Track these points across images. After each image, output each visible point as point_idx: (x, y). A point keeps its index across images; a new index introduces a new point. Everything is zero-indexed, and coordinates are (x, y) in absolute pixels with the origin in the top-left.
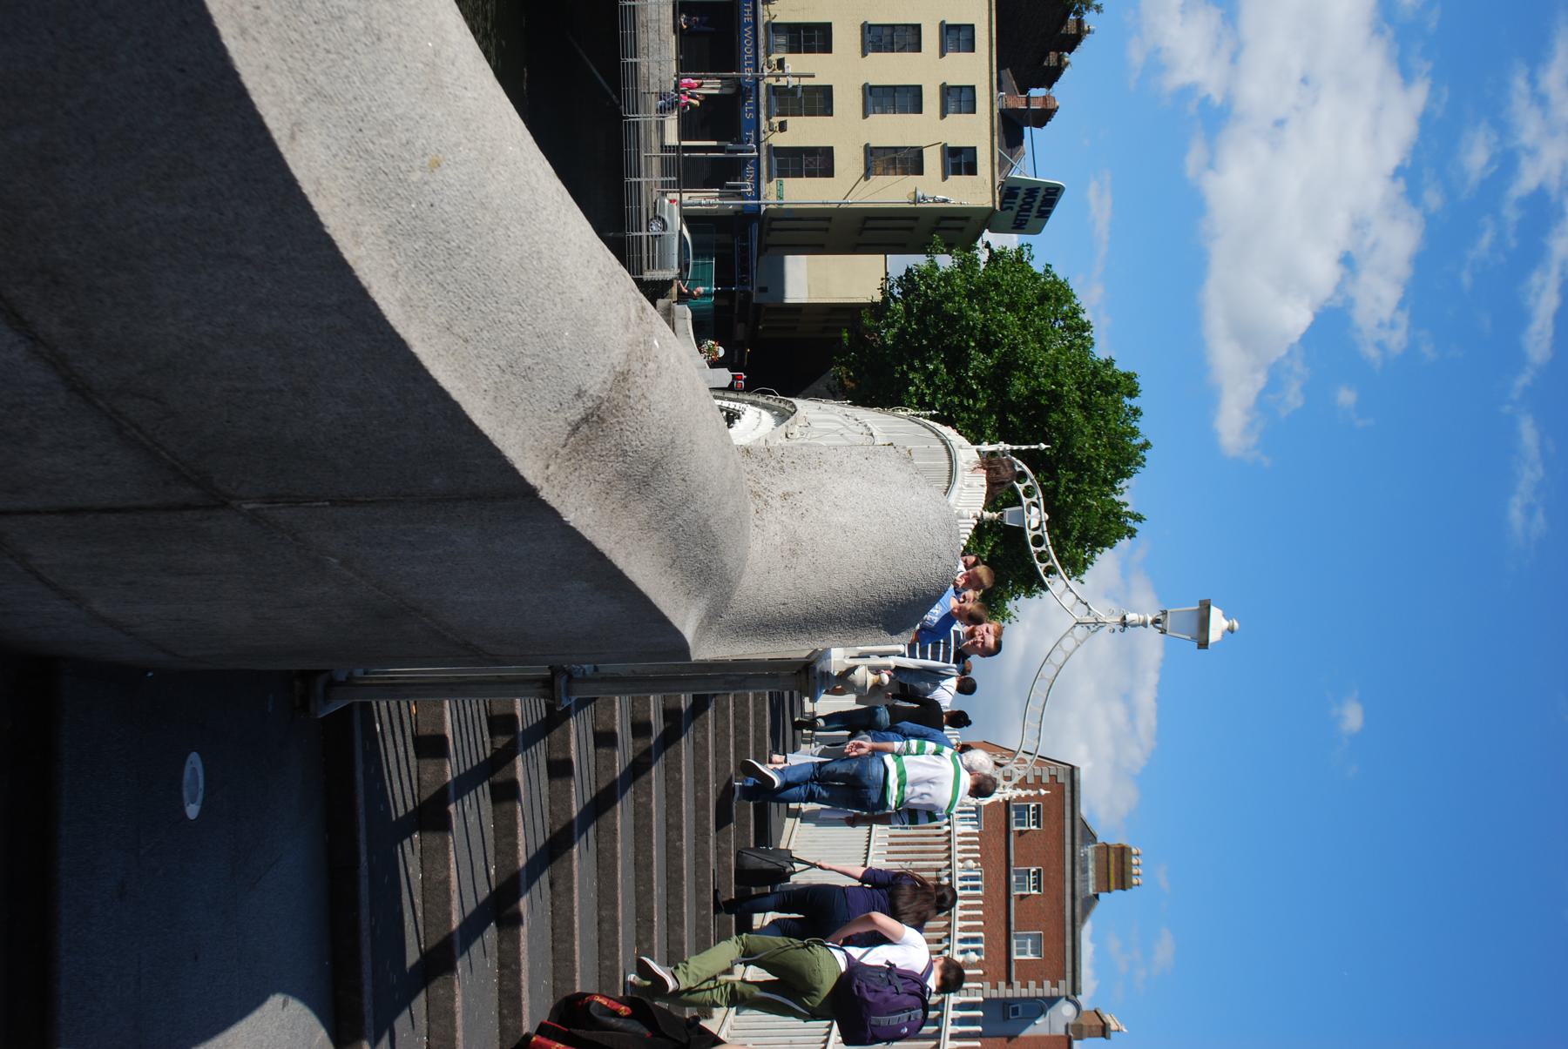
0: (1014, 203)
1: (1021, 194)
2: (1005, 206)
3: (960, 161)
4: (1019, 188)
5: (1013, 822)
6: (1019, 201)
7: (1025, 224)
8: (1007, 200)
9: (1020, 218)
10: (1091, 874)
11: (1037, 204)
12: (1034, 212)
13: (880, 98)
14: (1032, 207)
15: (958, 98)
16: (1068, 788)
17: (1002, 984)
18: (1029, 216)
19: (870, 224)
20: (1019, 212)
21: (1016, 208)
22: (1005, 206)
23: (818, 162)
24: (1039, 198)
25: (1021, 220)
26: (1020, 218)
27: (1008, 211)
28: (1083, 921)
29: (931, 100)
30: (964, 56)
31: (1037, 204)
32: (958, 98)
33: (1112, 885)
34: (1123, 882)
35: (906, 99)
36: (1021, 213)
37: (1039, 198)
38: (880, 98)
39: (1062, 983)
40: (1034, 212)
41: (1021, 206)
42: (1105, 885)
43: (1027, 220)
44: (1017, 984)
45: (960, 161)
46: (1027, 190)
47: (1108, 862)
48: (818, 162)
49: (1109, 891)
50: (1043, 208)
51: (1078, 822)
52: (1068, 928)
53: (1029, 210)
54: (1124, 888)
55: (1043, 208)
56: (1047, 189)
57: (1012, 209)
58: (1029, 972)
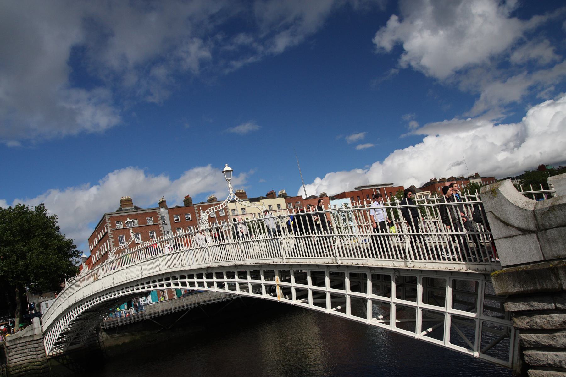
5: (122, 228)
10: (129, 208)
16: (111, 216)
17: (160, 226)
28: (141, 209)
33: (131, 203)
34: (130, 200)
39: (157, 212)
42: (131, 204)
44: (159, 222)
47: (126, 204)
49: (133, 203)
51: (117, 212)
52: (144, 212)
54: (131, 200)
58: (156, 220)
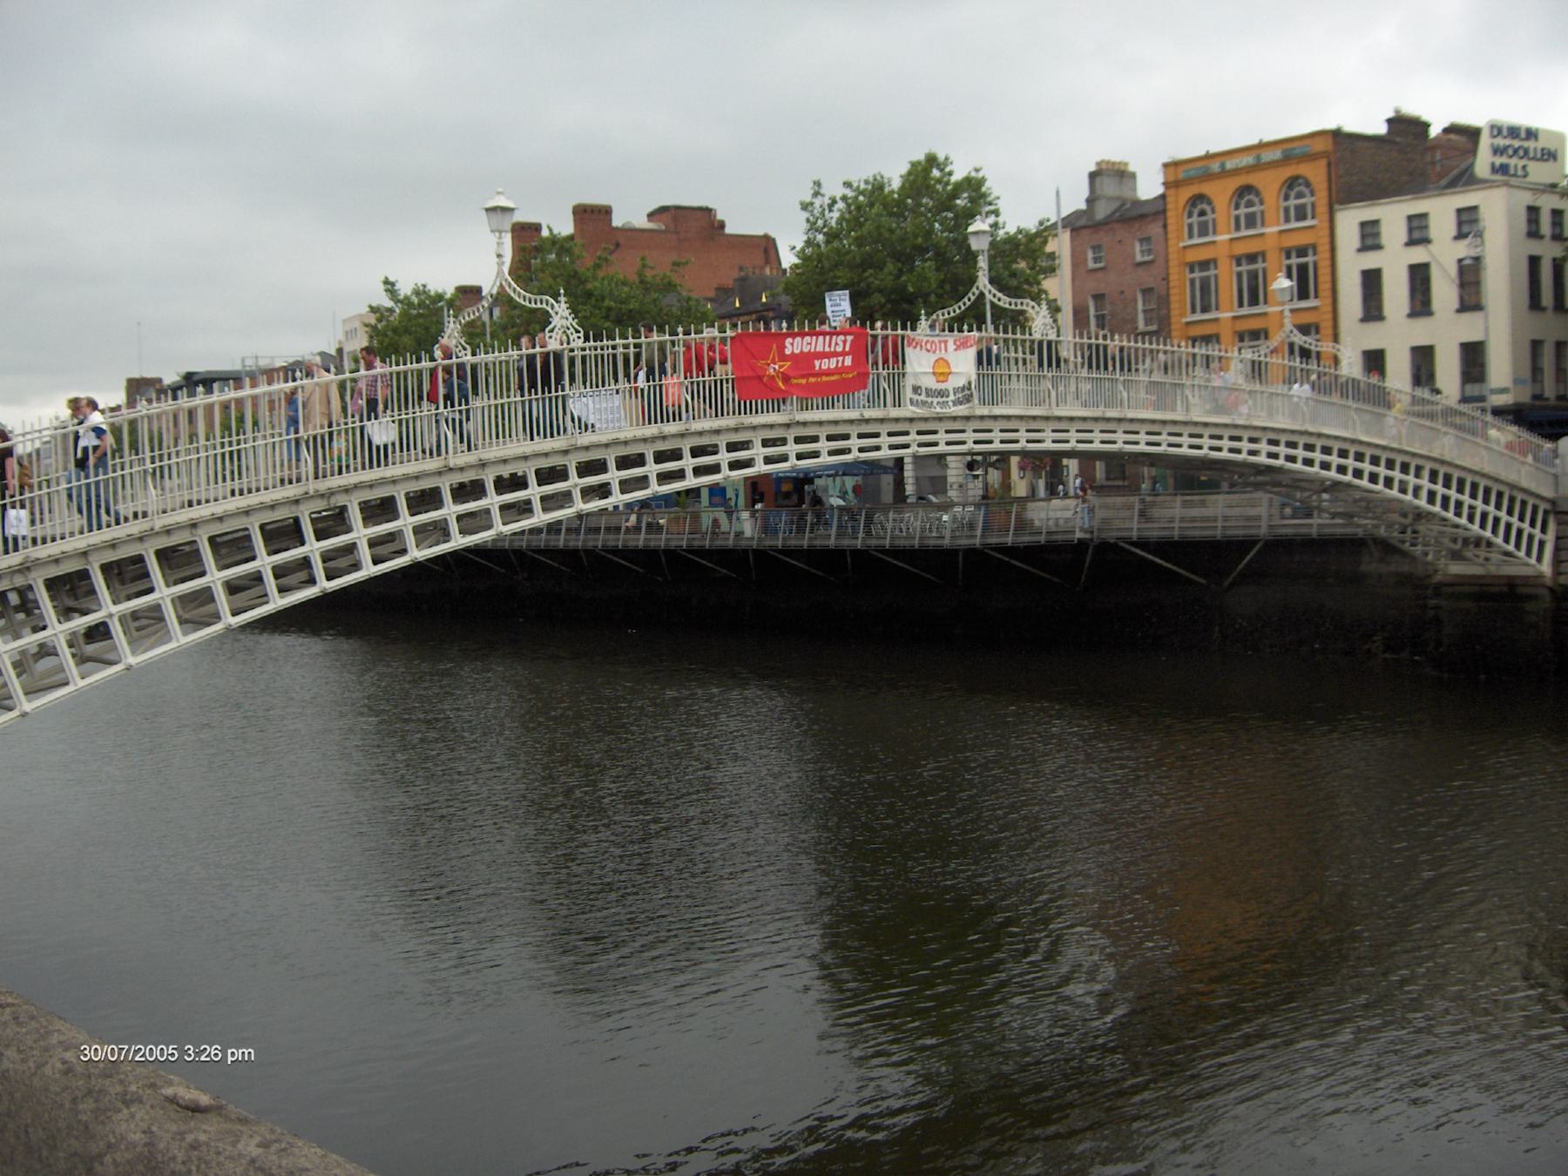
1: (1499, 160)
2: (1520, 172)
3: (1467, 222)
6: (1513, 162)
11: (1516, 143)
13: (1421, 303)
15: (1418, 232)
19: (1547, 297)
21: (1524, 162)
23: (1473, 357)
24: (1507, 142)
27: (1528, 169)
29: (1418, 255)
31: (1516, 143)
32: (1418, 232)
35: (1420, 277)
37: (1501, 142)
38: (1421, 303)
40: (1531, 144)
43: (1543, 150)
45: (1467, 222)
48: (1473, 357)
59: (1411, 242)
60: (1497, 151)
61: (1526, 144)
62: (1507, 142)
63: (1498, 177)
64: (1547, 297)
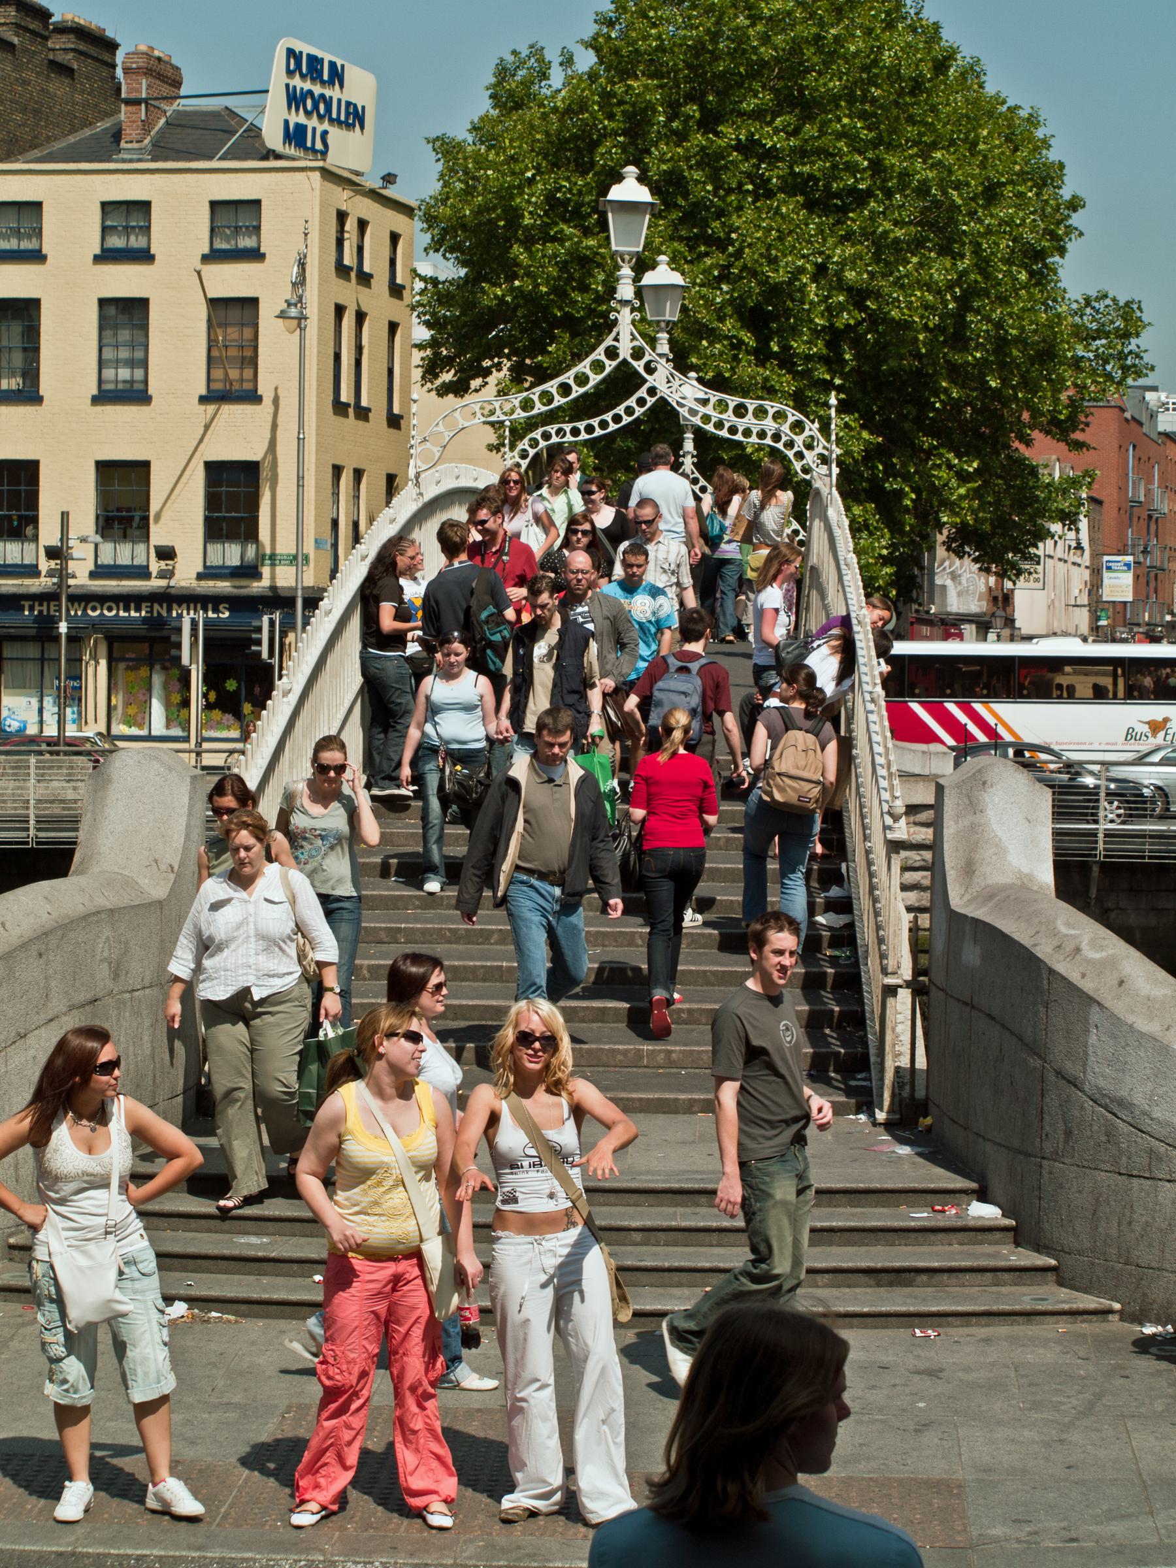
0: (314, 129)
2: (319, 146)
4: (286, 122)
6: (312, 123)
7: (355, 106)
8: (309, 144)
9: (343, 118)
11: (317, 90)
12: (333, 93)
14: (322, 96)
18: (339, 101)
19: (346, 396)
20: (331, 121)
21: (326, 126)
22: (319, 146)
24: (307, 85)
25: (348, 114)
26: (343, 118)
27: (330, 141)
30: (50, 220)
31: (317, 90)
36: (334, 115)
40: (333, 93)
41: (321, 118)
43: (348, 104)
46: (289, 107)
50: (326, 77)
53: (328, 103)
55: (326, 77)
56: (290, 73)
57: (325, 134)
59: (106, 256)
60: (295, 99)
61: (328, 93)
62: (307, 85)
63: (291, 151)
64: (346, 396)
